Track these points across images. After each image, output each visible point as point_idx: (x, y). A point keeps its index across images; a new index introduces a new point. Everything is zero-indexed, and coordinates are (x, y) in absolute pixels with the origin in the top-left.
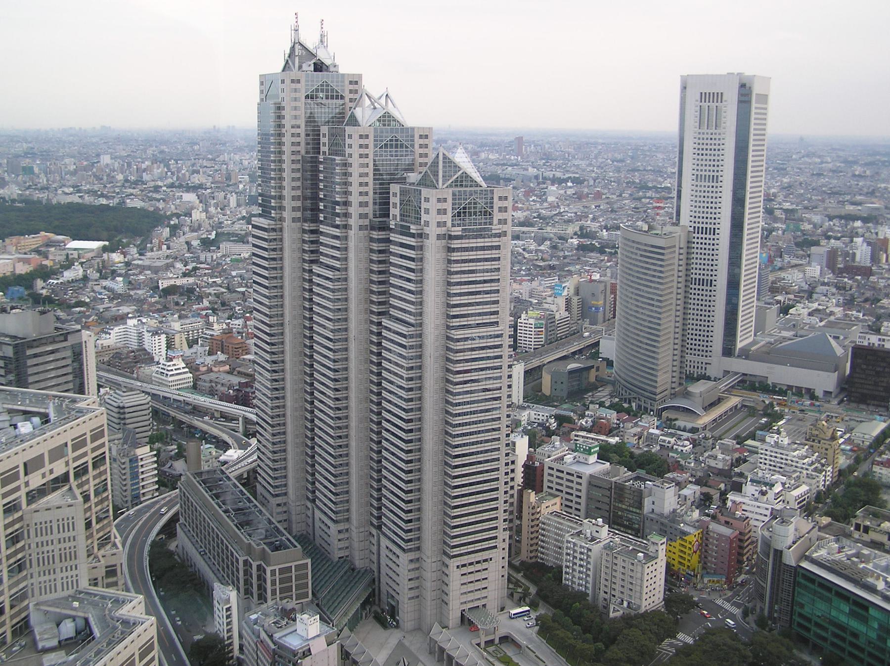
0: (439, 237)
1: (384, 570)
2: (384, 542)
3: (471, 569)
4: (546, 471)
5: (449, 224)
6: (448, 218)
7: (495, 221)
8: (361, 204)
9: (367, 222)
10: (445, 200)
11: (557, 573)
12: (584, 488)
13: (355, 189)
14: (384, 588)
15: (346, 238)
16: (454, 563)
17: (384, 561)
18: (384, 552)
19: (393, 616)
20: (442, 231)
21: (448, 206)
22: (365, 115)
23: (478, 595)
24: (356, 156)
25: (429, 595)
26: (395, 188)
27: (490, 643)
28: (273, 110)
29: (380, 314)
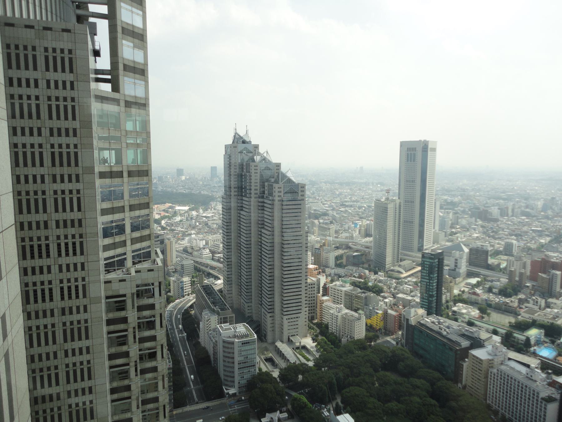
0: (279, 201)
1: (263, 321)
2: (263, 310)
3: (292, 320)
4: (330, 289)
5: (282, 196)
6: (282, 194)
7: (300, 195)
8: (255, 190)
9: (257, 196)
10: (281, 188)
11: (327, 326)
12: (343, 295)
13: (253, 184)
14: (263, 328)
15: (250, 201)
16: (285, 317)
17: (263, 317)
18: (263, 314)
19: (265, 338)
20: (280, 198)
21: (282, 190)
22: (257, 158)
23: (295, 330)
24: (253, 173)
25: (277, 330)
26: (266, 184)
27: (298, 348)
28: (229, 157)
29: (262, 228)
